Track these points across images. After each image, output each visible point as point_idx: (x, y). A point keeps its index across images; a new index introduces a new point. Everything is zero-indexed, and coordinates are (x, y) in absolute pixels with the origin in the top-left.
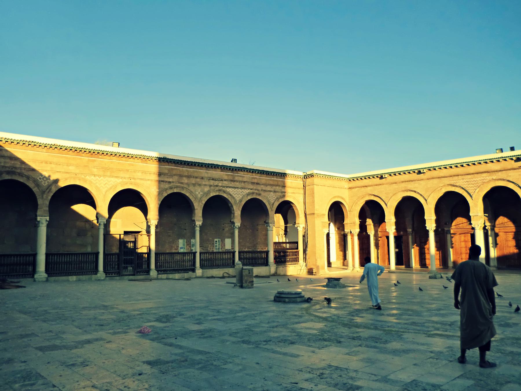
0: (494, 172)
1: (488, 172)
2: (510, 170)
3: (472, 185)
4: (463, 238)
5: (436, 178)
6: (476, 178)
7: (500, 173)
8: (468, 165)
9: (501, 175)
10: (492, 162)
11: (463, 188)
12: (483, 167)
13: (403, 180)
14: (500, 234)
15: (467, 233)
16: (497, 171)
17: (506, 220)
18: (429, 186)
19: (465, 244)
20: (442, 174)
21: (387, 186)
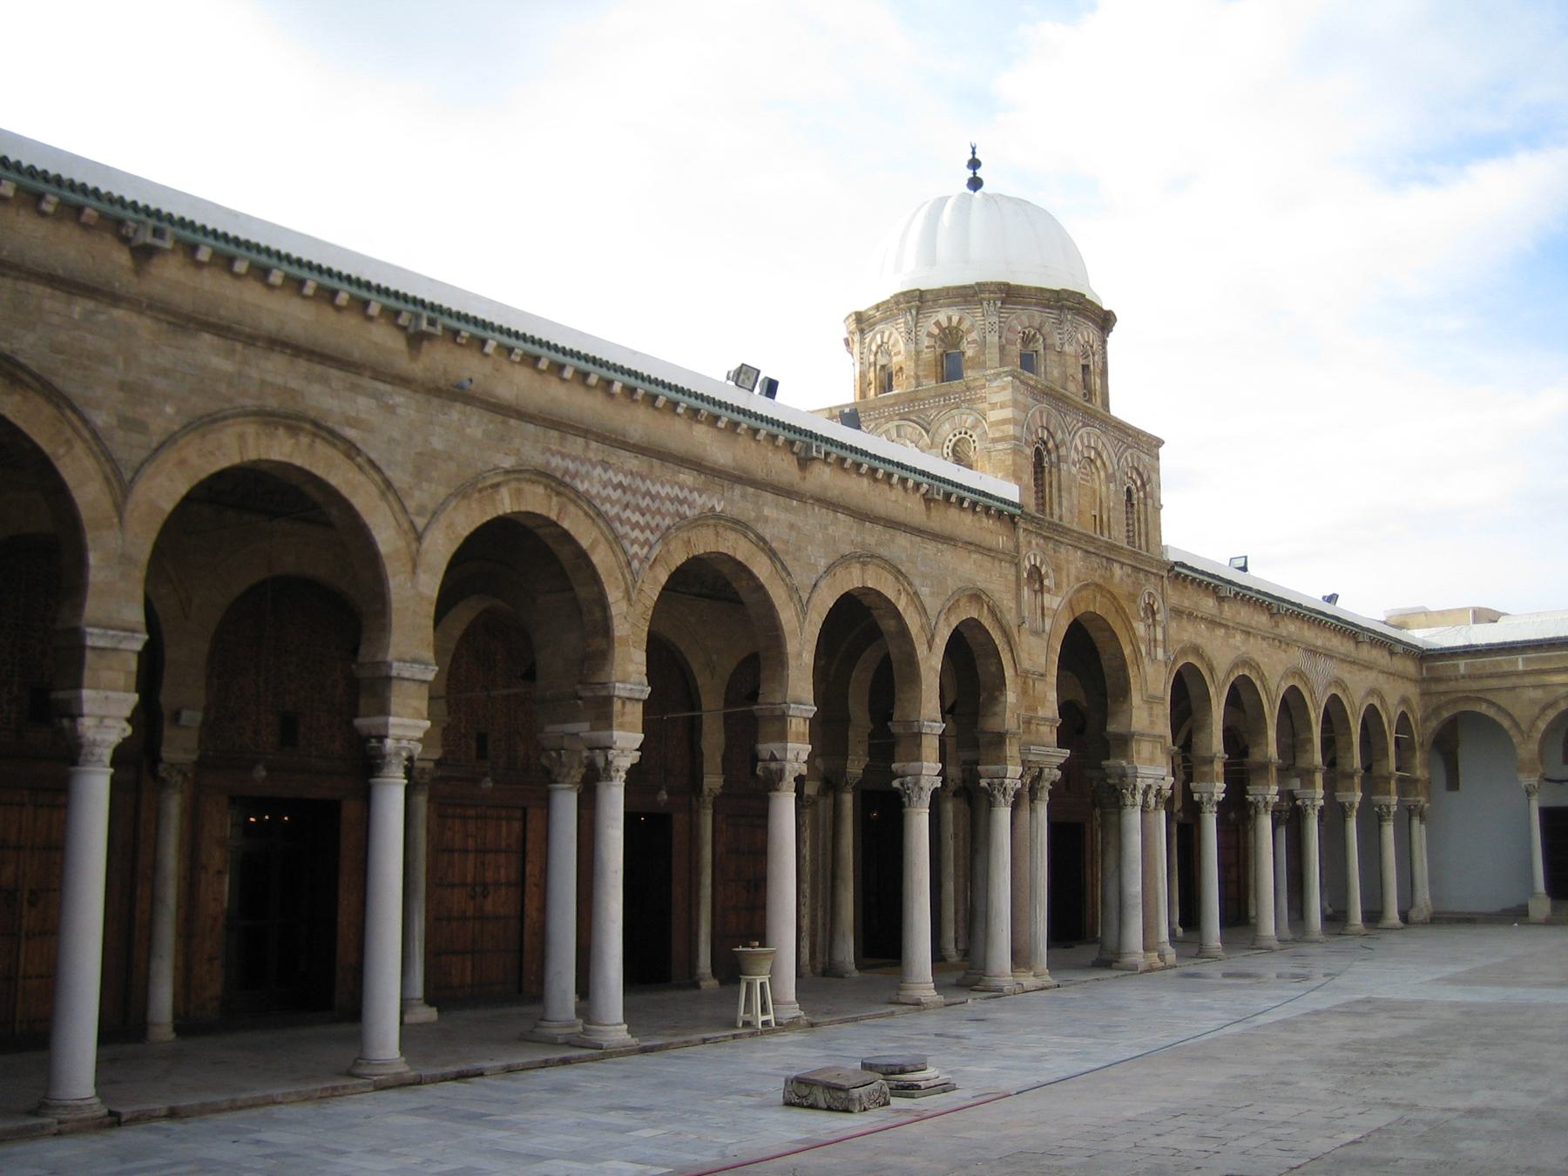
3: (636, 517)
8: (630, 391)
13: (269, 324)
18: (437, 443)
21: (144, 325)
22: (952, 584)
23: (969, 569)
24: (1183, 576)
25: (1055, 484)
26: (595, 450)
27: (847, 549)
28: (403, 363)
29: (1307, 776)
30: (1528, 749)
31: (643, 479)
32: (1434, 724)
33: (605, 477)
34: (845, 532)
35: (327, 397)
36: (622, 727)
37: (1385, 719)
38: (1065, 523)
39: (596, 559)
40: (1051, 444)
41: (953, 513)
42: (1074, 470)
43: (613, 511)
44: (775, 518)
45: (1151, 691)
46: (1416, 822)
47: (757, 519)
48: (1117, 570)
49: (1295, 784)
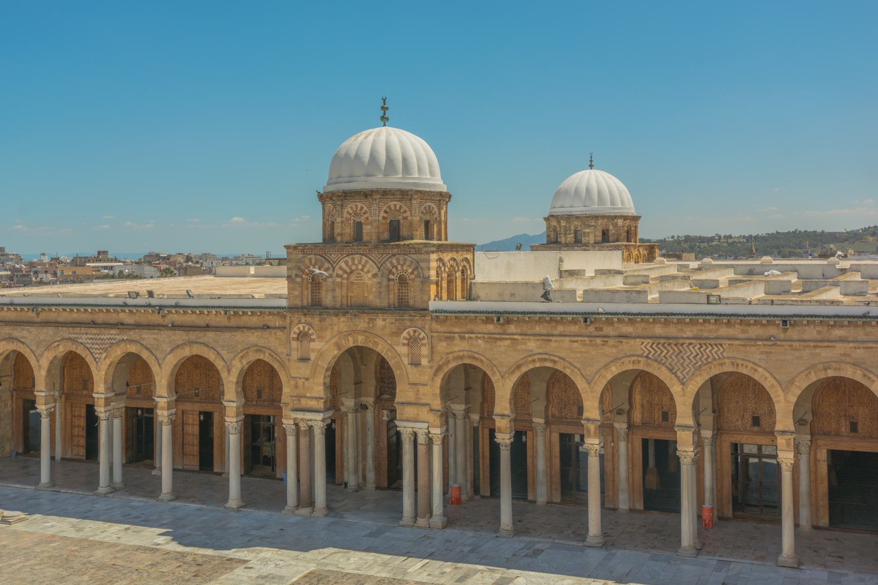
9: (133, 334)
13: (7, 319)
18: (41, 338)
20: (60, 319)
22: (240, 347)
23: (253, 338)
24: (440, 316)
25: (324, 288)
26: (83, 330)
27: (181, 343)
28: (36, 320)
34: (179, 336)
35: (17, 333)
39: (87, 360)
42: (338, 280)
44: (148, 337)
45: (412, 380)
48: (380, 322)
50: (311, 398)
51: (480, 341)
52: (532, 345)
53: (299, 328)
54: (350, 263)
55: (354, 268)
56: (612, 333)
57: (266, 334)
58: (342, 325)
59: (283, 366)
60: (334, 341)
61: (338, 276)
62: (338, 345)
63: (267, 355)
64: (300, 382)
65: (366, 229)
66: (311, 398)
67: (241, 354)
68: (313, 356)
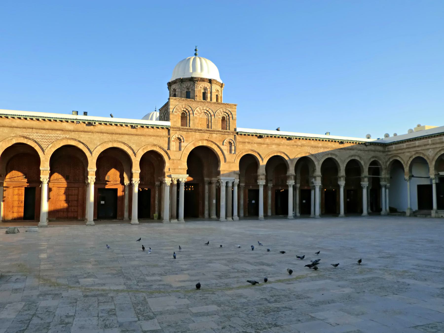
0: (68, 131)
1: (62, 130)
2: (81, 131)
3: (47, 141)
4: (16, 191)
5: (8, 127)
6: (51, 134)
7: (73, 133)
8: (44, 120)
9: (73, 135)
10: (67, 122)
11: (36, 142)
12: (58, 125)
14: (53, 189)
15: (22, 187)
16: (70, 131)
17: (60, 176)
19: (18, 198)
20: (14, 124)
22: (143, 144)
23: (151, 140)
27: (107, 140)
29: (315, 177)
30: (407, 169)
31: (47, 134)
32: (388, 163)
33: (37, 135)
34: (106, 137)
36: (43, 175)
37: (362, 163)
38: (191, 127)
40: (187, 111)
41: (146, 130)
43: (39, 140)
46: (383, 189)
47: (79, 137)
48: (214, 135)
49: (313, 180)
50: (181, 169)
51: (255, 145)
52: (274, 147)
53: (176, 136)
54: (202, 109)
55: (203, 111)
56: (300, 144)
57: (158, 138)
58: (197, 136)
59: (167, 153)
60: (193, 142)
61: (196, 114)
62: (194, 144)
63: (158, 147)
64: (175, 161)
65: (209, 95)
66: (181, 169)
67: (144, 147)
68: (182, 149)
